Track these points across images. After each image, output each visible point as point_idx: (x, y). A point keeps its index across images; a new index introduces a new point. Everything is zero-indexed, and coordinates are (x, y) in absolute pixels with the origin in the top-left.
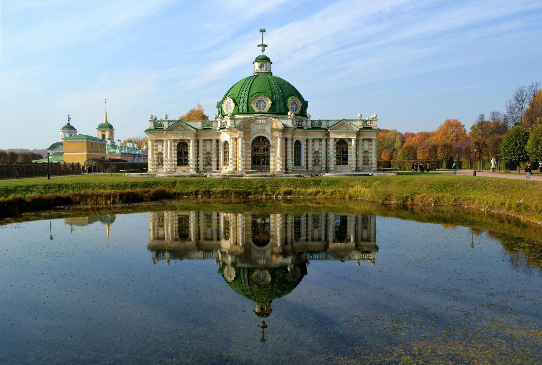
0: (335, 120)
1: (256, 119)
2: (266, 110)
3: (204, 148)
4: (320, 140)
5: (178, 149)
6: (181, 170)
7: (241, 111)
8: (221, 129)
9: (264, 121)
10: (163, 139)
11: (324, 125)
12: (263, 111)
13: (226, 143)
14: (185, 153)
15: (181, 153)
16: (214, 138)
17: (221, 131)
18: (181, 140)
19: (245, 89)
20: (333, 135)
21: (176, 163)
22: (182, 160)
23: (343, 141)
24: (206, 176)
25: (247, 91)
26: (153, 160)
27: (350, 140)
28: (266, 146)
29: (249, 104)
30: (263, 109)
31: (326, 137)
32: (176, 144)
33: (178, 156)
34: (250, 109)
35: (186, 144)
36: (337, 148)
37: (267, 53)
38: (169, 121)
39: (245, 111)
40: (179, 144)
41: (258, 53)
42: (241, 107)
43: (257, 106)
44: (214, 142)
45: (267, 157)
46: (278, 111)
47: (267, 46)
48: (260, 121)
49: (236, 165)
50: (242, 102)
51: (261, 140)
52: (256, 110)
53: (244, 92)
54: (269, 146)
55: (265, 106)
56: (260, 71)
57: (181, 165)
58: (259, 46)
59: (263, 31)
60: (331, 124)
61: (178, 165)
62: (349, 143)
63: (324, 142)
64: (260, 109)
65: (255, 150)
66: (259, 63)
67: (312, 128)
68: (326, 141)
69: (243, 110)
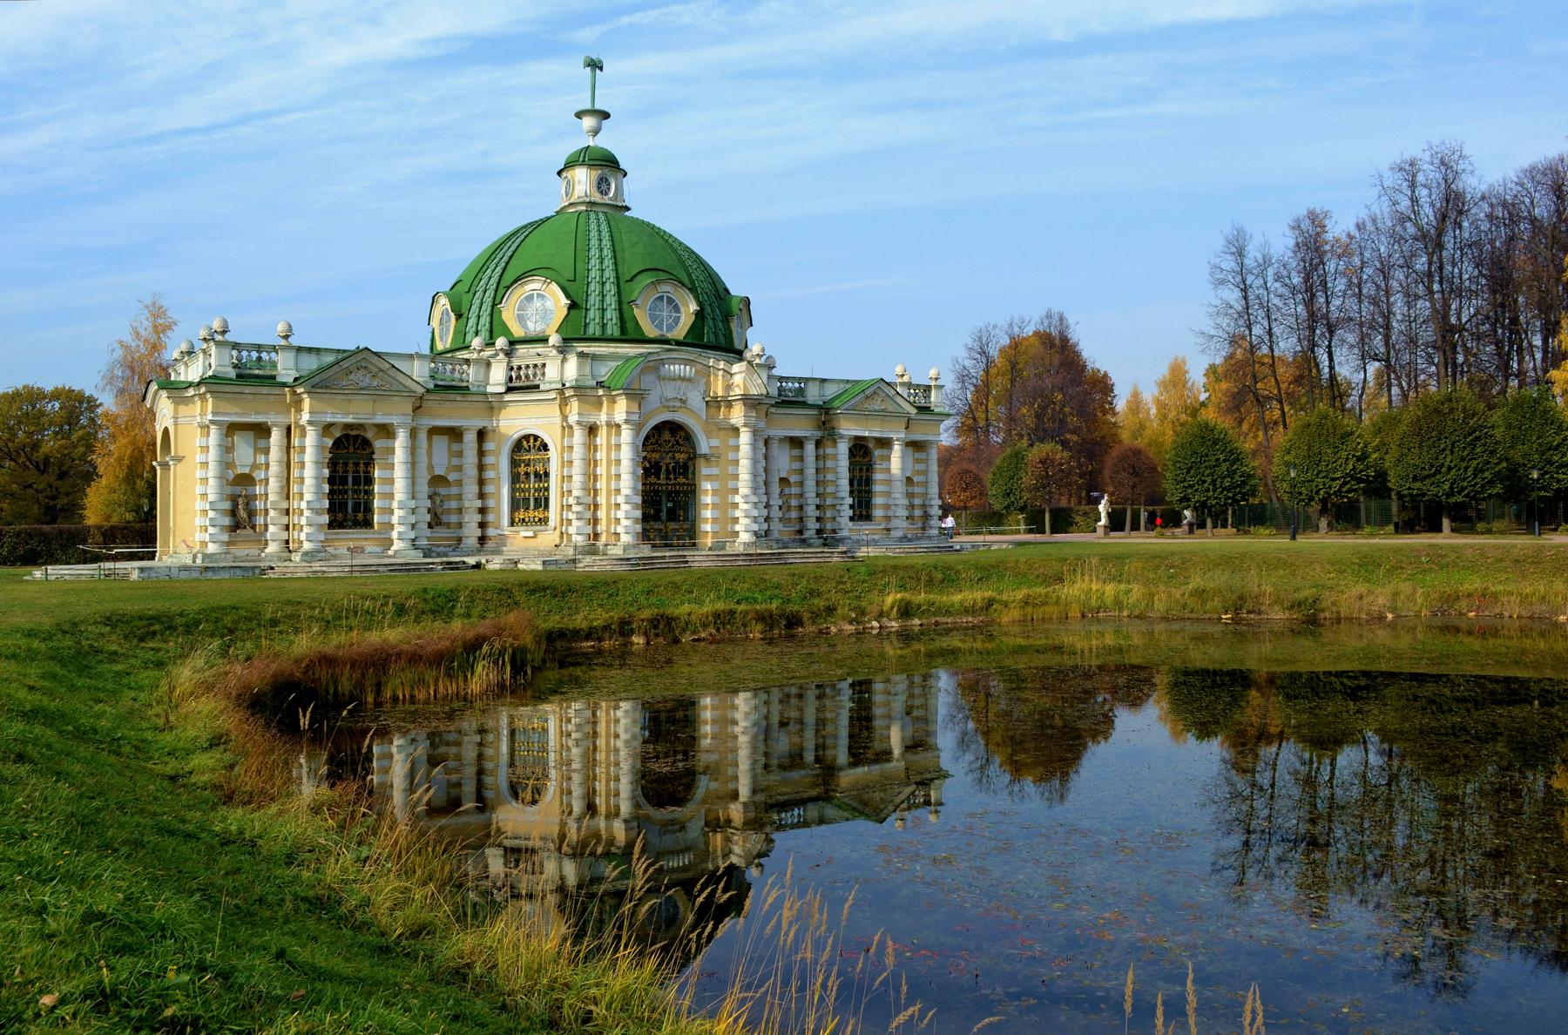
0: (841, 381)
1: (662, 362)
2: (680, 332)
3: (455, 461)
4: (797, 443)
5: (333, 464)
6: (351, 551)
7: (594, 329)
8: (510, 390)
9: (687, 370)
11: (813, 394)
12: (669, 335)
13: (528, 445)
14: (356, 481)
15: (344, 481)
16: (471, 422)
17: (508, 397)
18: (348, 426)
19: (594, 252)
20: (850, 428)
21: (326, 519)
22: (349, 501)
23: (862, 446)
24: (478, 566)
25: (608, 262)
26: (413, 504)
28: (681, 457)
29: (625, 306)
30: (670, 328)
31: (819, 434)
32: (329, 442)
33: (369, 493)
34: (630, 326)
35: (366, 444)
37: (607, 141)
38: (299, 349)
39: (613, 329)
40: (337, 443)
41: (581, 136)
42: (593, 314)
43: (653, 319)
44: (470, 438)
45: (686, 493)
46: (598, 334)
47: (606, 115)
48: (675, 369)
51: (667, 435)
52: (650, 331)
53: (594, 262)
54: (693, 456)
56: (597, 197)
57: (341, 525)
58: (579, 115)
60: (831, 391)
61: (331, 526)
62: (877, 453)
63: (810, 448)
64: (659, 326)
65: (650, 470)
66: (596, 173)
67: (784, 402)
68: (818, 444)
69: (604, 326)
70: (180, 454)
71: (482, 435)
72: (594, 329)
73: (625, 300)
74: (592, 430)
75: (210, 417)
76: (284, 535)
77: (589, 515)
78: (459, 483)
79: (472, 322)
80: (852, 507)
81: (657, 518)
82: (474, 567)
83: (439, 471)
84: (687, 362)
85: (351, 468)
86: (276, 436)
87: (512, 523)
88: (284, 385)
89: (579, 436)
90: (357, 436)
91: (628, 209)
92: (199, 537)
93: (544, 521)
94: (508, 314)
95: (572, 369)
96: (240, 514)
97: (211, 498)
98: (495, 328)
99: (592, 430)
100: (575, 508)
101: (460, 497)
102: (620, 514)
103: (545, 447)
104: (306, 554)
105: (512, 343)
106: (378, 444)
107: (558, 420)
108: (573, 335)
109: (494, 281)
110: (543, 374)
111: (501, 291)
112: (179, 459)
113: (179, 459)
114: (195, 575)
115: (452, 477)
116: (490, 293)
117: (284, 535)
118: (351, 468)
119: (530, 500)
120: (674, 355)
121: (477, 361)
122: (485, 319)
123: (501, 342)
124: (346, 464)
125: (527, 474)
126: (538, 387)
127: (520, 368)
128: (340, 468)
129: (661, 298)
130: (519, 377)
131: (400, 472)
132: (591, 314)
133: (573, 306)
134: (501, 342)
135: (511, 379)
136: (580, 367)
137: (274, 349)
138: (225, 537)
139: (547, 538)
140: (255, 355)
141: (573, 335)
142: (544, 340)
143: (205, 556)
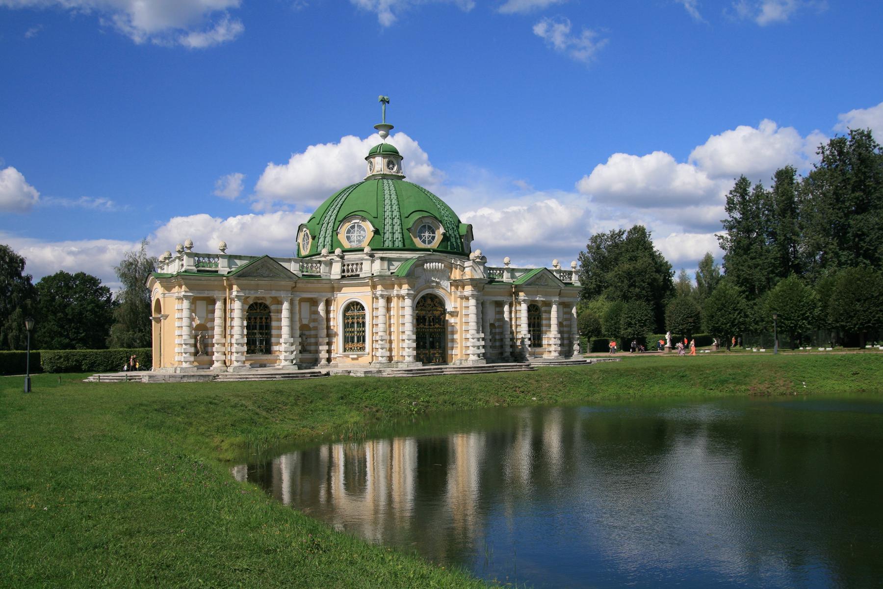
2: (435, 244)
10: (216, 294)
12: (429, 246)
13: (354, 306)
18: (258, 298)
21: (245, 348)
23: (534, 306)
24: (328, 374)
25: (395, 207)
27: (549, 305)
30: (430, 242)
32: (247, 307)
34: (407, 242)
35: (266, 307)
36: (249, 319)
39: (398, 244)
45: (440, 333)
48: (433, 265)
49: (390, 350)
50: (388, 227)
51: (429, 301)
53: (388, 207)
55: (433, 238)
56: (387, 172)
59: (383, 101)
61: (248, 352)
62: (543, 309)
64: (424, 242)
65: (419, 320)
66: (386, 160)
69: (394, 242)
70: (167, 313)
71: (328, 303)
72: (388, 244)
73: (405, 228)
74: (389, 300)
75: (183, 293)
76: (223, 358)
77: (387, 346)
78: (316, 328)
79: (321, 240)
80: (530, 339)
81: (424, 347)
82: (325, 375)
83: (305, 322)
84: (438, 261)
85: (258, 321)
86: (219, 305)
87: (345, 350)
88: (223, 276)
89: (382, 303)
90: (261, 304)
91: (404, 177)
92: (177, 358)
93: (363, 349)
94: (342, 237)
95: (377, 267)
96: (201, 346)
97: (184, 337)
98: (334, 244)
99: (389, 300)
100: (380, 342)
101: (316, 336)
102: (405, 345)
103: (363, 308)
104: (235, 368)
105: (343, 251)
106: (273, 307)
107: (370, 294)
108: (378, 246)
109: (333, 217)
110: (361, 269)
111: (337, 223)
112: (166, 317)
113: (166, 317)
114: (178, 379)
115: (311, 325)
116: (331, 224)
117: (223, 358)
118: (258, 321)
119: (355, 336)
120: (432, 257)
121: (326, 263)
122: (328, 239)
123: (338, 251)
124: (255, 318)
125: (353, 323)
126: (358, 275)
127: (348, 265)
128: (252, 321)
129: (424, 226)
130: (348, 271)
131: (285, 323)
132: (387, 236)
133: (376, 232)
134: (338, 251)
135: (343, 271)
136: (382, 265)
137: (217, 256)
138: (192, 359)
139: (365, 360)
140: (206, 259)
141: (378, 246)
142: (363, 250)
143: (182, 369)
